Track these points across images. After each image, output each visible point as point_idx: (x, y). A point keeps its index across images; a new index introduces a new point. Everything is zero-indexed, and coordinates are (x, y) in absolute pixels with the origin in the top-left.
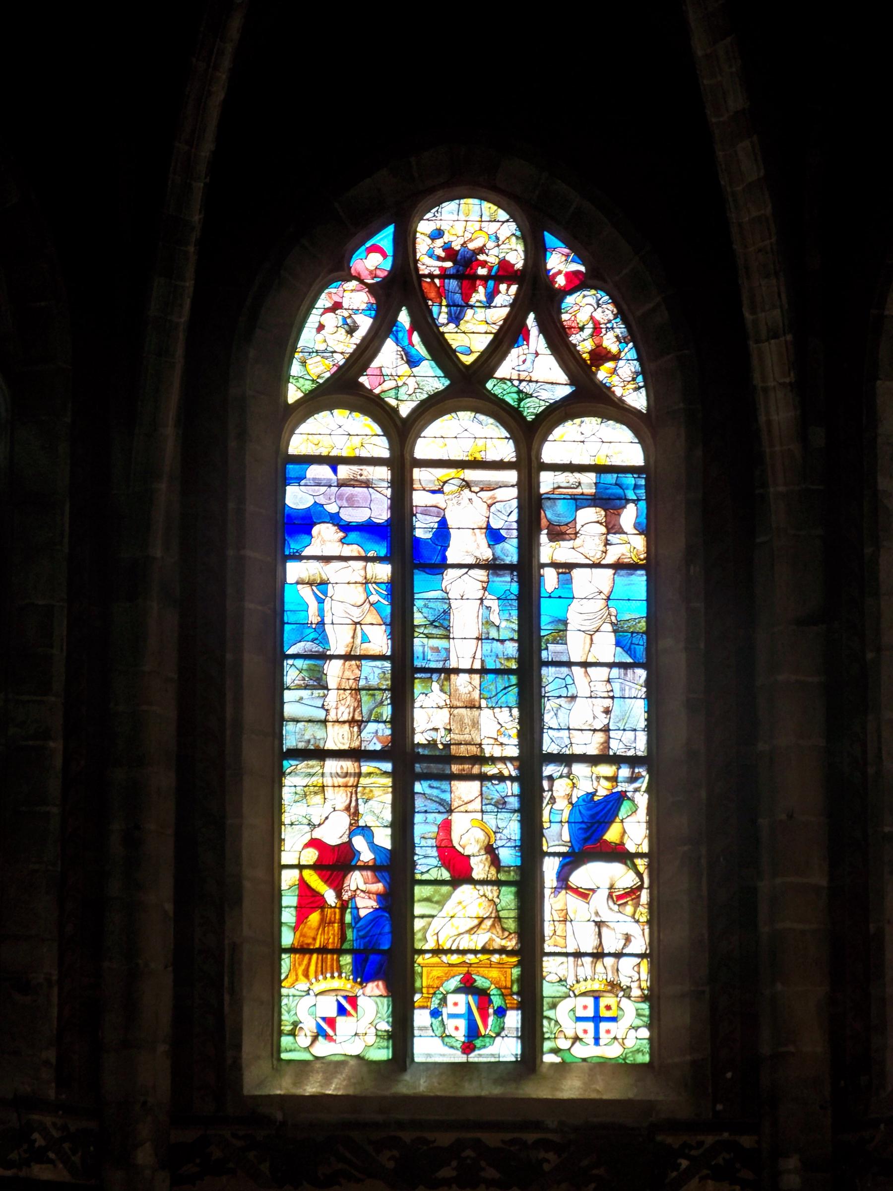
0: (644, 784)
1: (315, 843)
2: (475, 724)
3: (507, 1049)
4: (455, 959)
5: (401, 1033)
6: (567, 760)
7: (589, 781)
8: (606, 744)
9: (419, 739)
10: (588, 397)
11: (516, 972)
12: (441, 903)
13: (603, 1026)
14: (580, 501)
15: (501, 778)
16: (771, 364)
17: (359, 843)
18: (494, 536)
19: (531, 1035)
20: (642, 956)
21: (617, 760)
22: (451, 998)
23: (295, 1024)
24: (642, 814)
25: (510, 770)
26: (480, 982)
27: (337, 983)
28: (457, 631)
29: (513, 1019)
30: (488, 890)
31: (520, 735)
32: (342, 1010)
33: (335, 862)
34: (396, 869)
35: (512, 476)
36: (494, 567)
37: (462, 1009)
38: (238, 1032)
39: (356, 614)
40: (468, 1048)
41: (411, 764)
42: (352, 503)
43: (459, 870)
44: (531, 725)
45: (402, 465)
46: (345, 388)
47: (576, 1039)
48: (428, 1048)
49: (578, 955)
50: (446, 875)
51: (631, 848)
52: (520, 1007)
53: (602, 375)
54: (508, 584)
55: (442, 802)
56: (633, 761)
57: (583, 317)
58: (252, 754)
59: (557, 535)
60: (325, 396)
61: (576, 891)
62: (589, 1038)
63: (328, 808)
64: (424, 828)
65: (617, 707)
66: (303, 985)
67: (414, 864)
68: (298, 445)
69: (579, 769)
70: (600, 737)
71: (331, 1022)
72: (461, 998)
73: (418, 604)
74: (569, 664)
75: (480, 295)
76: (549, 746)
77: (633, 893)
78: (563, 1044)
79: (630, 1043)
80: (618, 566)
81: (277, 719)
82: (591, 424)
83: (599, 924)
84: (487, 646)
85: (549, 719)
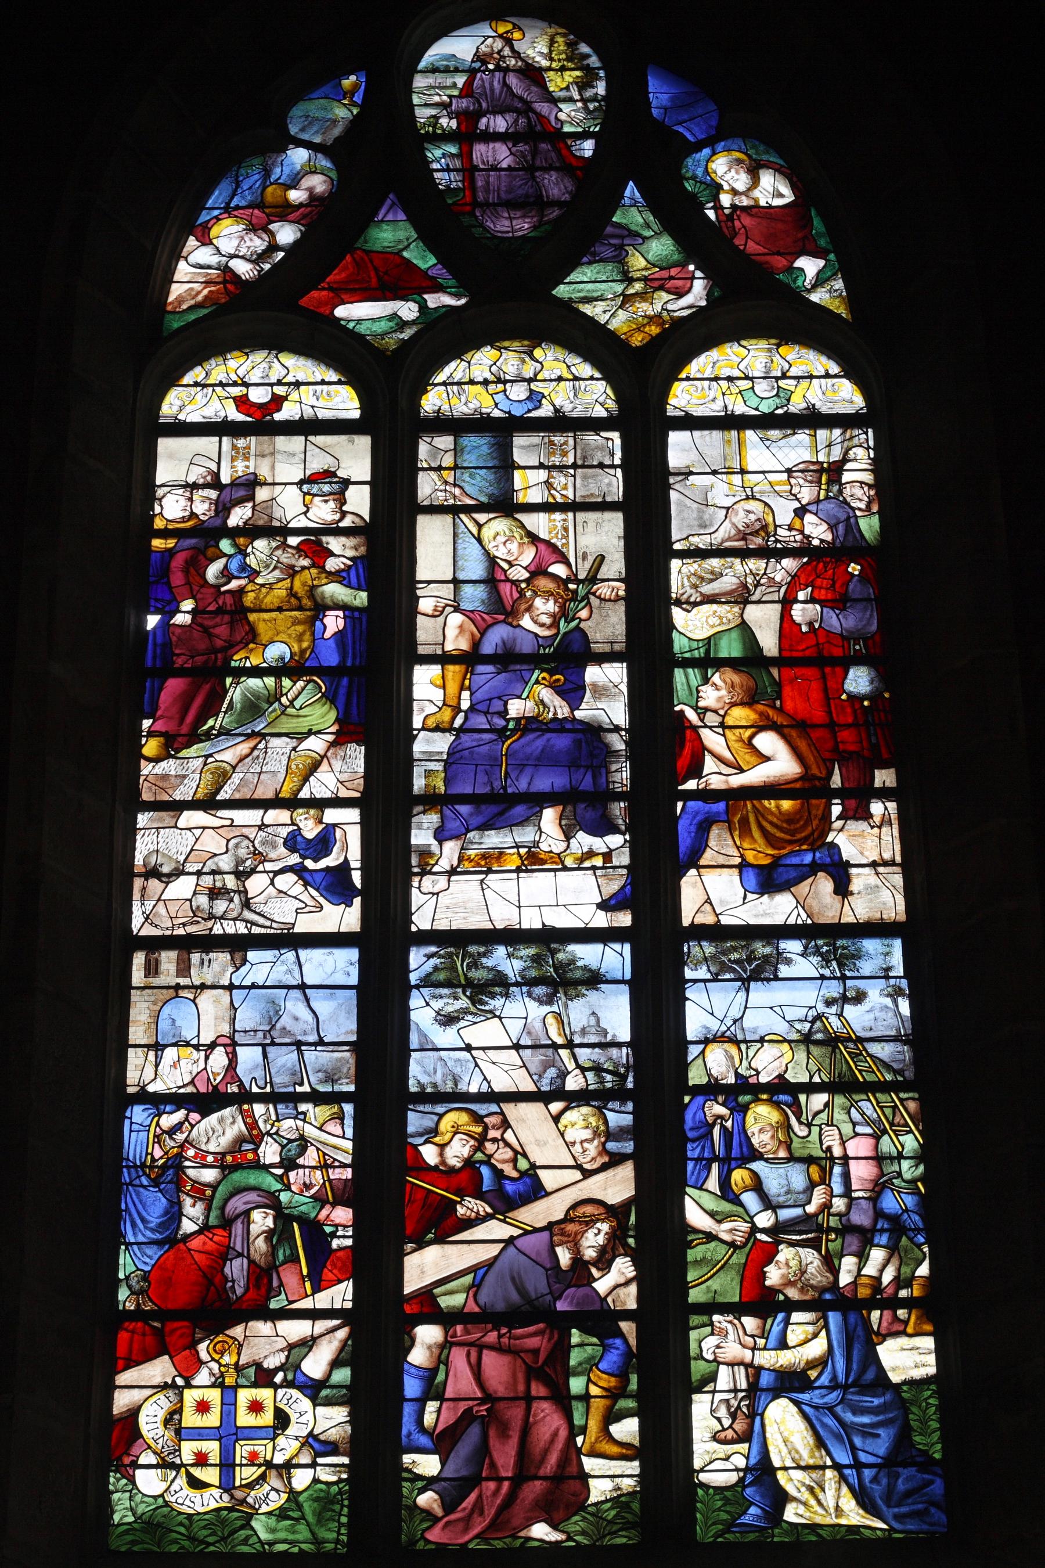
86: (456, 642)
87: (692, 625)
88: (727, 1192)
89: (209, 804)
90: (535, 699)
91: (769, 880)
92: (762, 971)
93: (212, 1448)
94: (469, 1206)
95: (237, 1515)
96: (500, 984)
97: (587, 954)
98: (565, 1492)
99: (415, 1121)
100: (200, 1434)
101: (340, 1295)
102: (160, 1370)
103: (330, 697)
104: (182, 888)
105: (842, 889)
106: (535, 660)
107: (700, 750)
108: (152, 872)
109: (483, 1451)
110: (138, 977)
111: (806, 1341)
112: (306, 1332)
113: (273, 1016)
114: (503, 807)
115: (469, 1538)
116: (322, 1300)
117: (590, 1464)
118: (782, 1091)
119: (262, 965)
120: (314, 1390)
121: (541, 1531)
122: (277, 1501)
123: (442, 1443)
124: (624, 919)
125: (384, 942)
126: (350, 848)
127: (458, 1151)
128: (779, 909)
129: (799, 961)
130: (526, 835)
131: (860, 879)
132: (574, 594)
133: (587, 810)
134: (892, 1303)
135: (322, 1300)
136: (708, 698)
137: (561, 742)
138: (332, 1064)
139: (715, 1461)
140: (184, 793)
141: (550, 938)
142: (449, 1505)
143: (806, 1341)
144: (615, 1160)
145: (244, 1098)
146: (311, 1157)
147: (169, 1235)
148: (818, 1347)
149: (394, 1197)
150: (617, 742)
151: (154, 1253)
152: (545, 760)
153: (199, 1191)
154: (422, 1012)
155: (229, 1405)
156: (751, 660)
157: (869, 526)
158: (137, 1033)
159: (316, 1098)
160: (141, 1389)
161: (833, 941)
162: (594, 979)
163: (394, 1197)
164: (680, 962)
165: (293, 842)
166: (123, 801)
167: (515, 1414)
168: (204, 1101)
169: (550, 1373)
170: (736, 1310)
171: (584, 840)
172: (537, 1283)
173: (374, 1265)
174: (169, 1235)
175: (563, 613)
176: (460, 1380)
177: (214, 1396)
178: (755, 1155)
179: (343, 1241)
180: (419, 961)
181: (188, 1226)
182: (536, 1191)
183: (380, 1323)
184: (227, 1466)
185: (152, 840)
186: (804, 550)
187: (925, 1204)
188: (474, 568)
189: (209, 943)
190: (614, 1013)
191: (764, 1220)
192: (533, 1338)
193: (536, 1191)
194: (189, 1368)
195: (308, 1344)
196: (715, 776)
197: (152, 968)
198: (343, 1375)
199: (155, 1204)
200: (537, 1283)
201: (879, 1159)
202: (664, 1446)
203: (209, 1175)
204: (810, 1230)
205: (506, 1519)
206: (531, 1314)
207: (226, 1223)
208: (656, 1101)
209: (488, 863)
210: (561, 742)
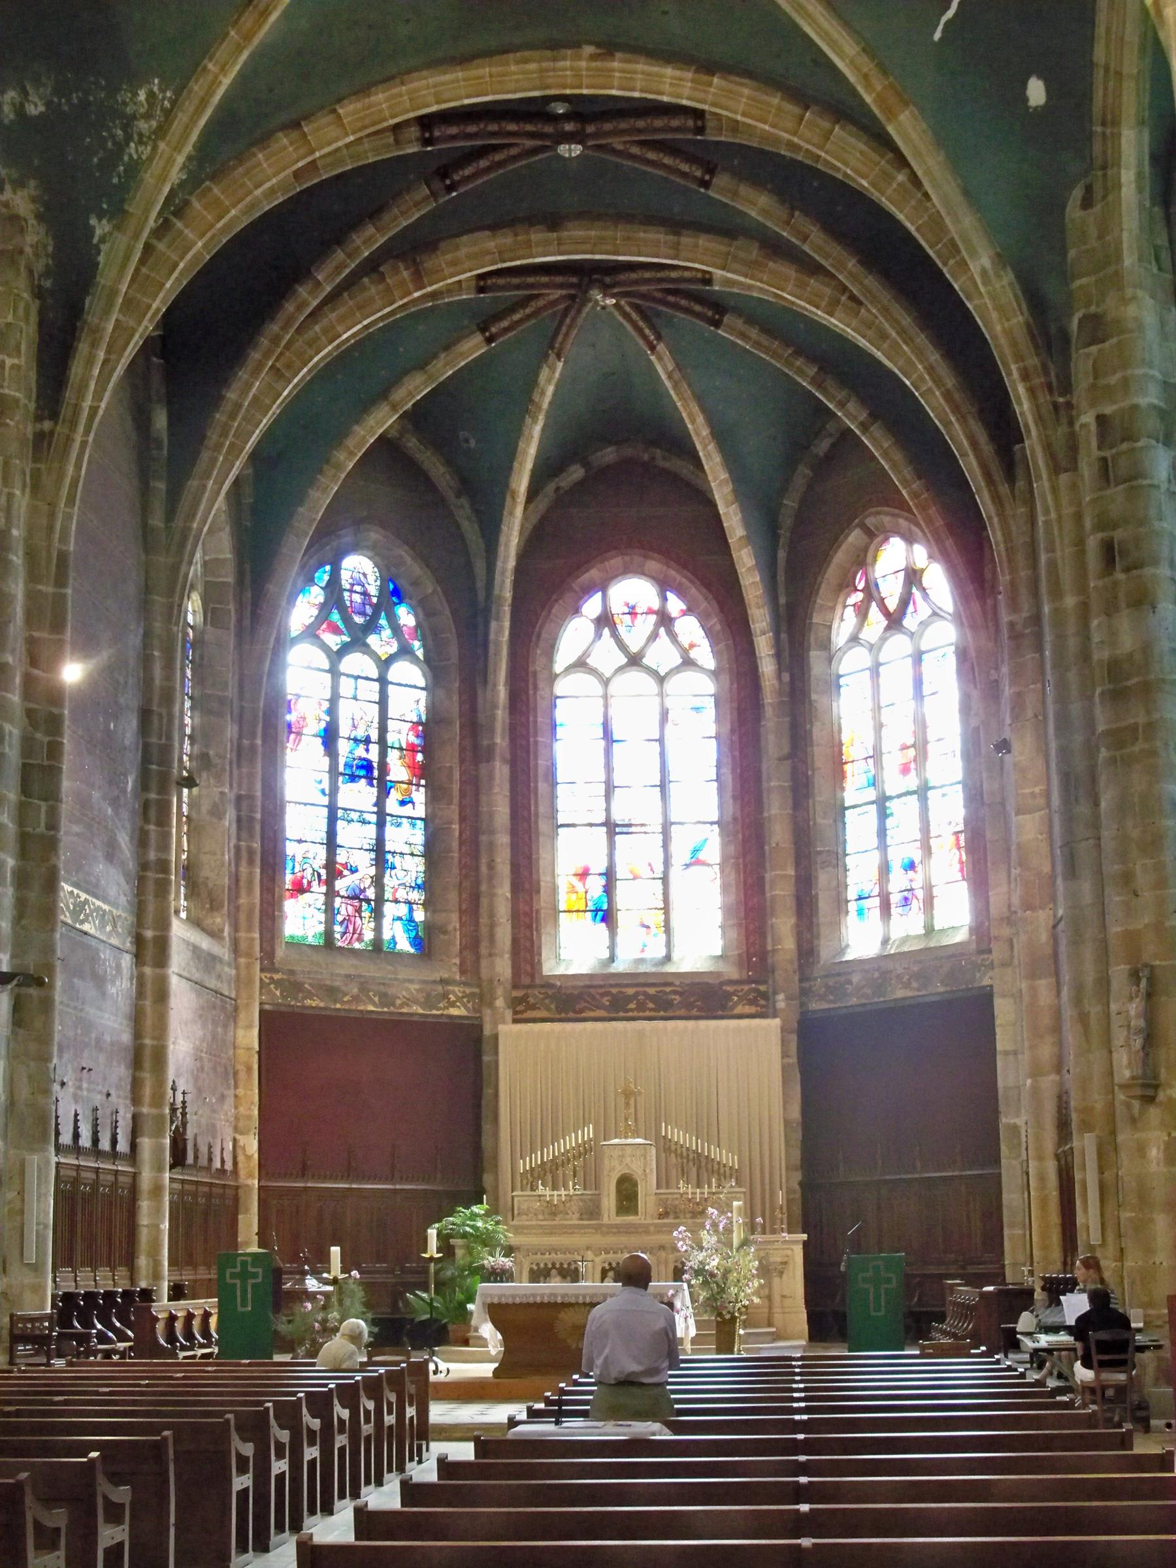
10: (688, 663)
16: (764, 646)
34: (610, 876)
38: (540, 948)
41: (612, 828)
46: (581, 664)
53: (693, 654)
58: (543, 826)
94: (346, 872)
111: (403, 910)
112: (316, 896)
114: (353, 778)
115: (344, 945)
136: (393, 757)
139: (386, 936)
143: (403, 910)
156: (401, 749)
169: (359, 910)
172: (357, 892)
173: (329, 883)
176: (343, 911)
180: (340, 813)
183: (331, 894)
190: (371, 831)
200: (357, 892)
202: (378, 929)
206: (356, 896)
208: (379, 850)
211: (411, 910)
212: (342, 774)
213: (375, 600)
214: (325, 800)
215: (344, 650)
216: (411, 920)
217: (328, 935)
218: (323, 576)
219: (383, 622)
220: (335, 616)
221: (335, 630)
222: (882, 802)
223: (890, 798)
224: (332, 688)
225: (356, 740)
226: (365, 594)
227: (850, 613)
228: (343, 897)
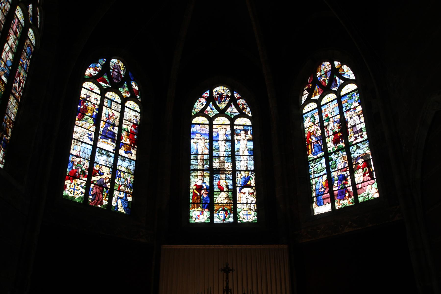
0: (254, 174)
1: (196, 185)
2: (224, 165)
3: (231, 220)
4: (221, 205)
5: (212, 218)
6: (240, 171)
7: (244, 174)
8: (247, 168)
9: (214, 167)
10: (242, 114)
11: (232, 207)
12: (219, 195)
13: (248, 216)
14: (241, 130)
15: (229, 174)
17: (204, 185)
18: (226, 135)
19: (235, 218)
20: (255, 204)
21: (249, 171)
22: (220, 212)
23: (192, 216)
24: (254, 180)
25: (230, 173)
26: (226, 209)
27: (200, 209)
28: (220, 150)
29: (232, 215)
30: (227, 193)
31: (232, 167)
32: (200, 214)
33: (199, 188)
34: (211, 190)
35: (229, 126)
36: (227, 140)
37: (223, 213)
39: (203, 148)
40: (224, 220)
42: (202, 130)
43: (222, 190)
44: (234, 166)
45: (211, 125)
46: (202, 113)
47: (243, 218)
48: (216, 220)
49: (243, 204)
50: (219, 190)
51: (252, 185)
52: (233, 213)
54: (229, 143)
55: (218, 178)
56: (252, 171)
57: (240, 103)
59: (237, 135)
60: (197, 115)
61: (242, 193)
62: (246, 218)
63: (198, 179)
64: (215, 182)
65: (249, 162)
66: (193, 210)
67: (214, 188)
68: (193, 122)
69: (242, 172)
70: (246, 167)
71: (199, 216)
72: (222, 212)
73: (214, 146)
74: (240, 155)
75: (224, 100)
76: (237, 169)
77: (253, 193)
78: (241, 219)
79: (253, 219)
80: (248, 140)
81: (189, 164)
82: (242, 118)
83: (247, 198)
84: (226, 153)
85: (237, 164)
86: (105, 120)
87: (124, 126)
88: (118, 180)
89: (81, 127)
90: (110, 128)
91: (126, 152)
92: (124, 161)
93: (73, 190)
94: (98, 174)
95: (74, 198)
96: (103, 154)
97: (111, 154)
98: (101, 203)
99: (95, 165)
100: (72, 189)
101: (86, 179)
102: (69, 181)
103: (93, 121)
104: (78, 135)
105: (131, 155)
106: (111, 124)
107: (122, 138)
108: (75, 132)
109: (95, 197)
110: (73, 142)
111: (122, 195)
112: (82, 181)
113: (84, 150)
114: (106, 137)
115: (93, 205)
116: (84, 179)
117: (104, 201)
118: (124, 172)
119: (84, 145)
120: (82, 187)
121: (99, 206)
122: (78, 197)
123: (92, 195)
124: (114, 152)
125: (95, 146)
126: (93, 136)
127: (98, 169)
128: (126, 155)
129: (127, 161)
130: (108, 141)
131: (133, 155)
132: (115, 119)
133: (113, 141)
134: (129, 194)
135: (84, 179)
136: (124, 133)
137: (112, 133)
138: (88, 156)
139: (114, 204)
140: (79, 125)
141: (108, 151)
142: (92, 201)
143: (122, 195)
144: (110, 174)
145: (80, 157)
146: (85, 165)
147: (72, 169)
148: (123, 196)
149: (91, 172)
150: (116, 135)
151: (70, 170)
152: (110, 134)
153: (75, 165)
154: (97, 154)
155: (75, 187)
156: (128, 132)
157: (139, 123)
158: (72, 148)
159: (86, 159)
160: (67, 182)
161: (130, 160)
162: (111, 157)
163: (91, 172)
164: (118, 157)
165: (88, 134)
166: (73, 124)
167: (99, 194)
168: (77, 156)
169: (102, 191)
170: (117, 191)
171: (112, 143)
172: (102, 183)
173: (89, 177)
174: (72, 169)
175: (114, 121)
176: (94, 190)
177: (74, 185)
178: (121, 177)
179: (87, 174)
180: (97, 150)
181: (74, 168)
182: (103, 175)
183: (89, 182)
184: (74, 192)
185: (76, 129)
186: (133, 123)
187: (133, 186)
188: (107, 114)
189: (80, 141)
190: (112, 160)
191: (121, 183)
192: (101, 188)
193: (103, 175)
194: (72, 182)
195: (82, 183)
196: (123, 141)
197: (74, 142)
198: (85, 187)
199: (71, 165)
200: (102, 183)
201: (130, 181)
202: (110, 201)
203: (76, 164)
204: (124, 185)
205: (96, 204)
207: (77, 169)
208: (114, 169)
209: (104, 142)
210: (112, 133)
211: (126, 196)
212: (100, 134)
213: (123, 76)
214: (92, 143)
215: (108, 90)
216: (126, 200)
217: (86, 197)
218: (102, 61)
219: (125, 85)
220: (105, 77)
221: (105, 82)
222: (327, 156)
223: (331, 154)
224: (101, 101)
225: (109, 123)
226: (119, 73)
227: (305, 92)
228: (94, 184)
